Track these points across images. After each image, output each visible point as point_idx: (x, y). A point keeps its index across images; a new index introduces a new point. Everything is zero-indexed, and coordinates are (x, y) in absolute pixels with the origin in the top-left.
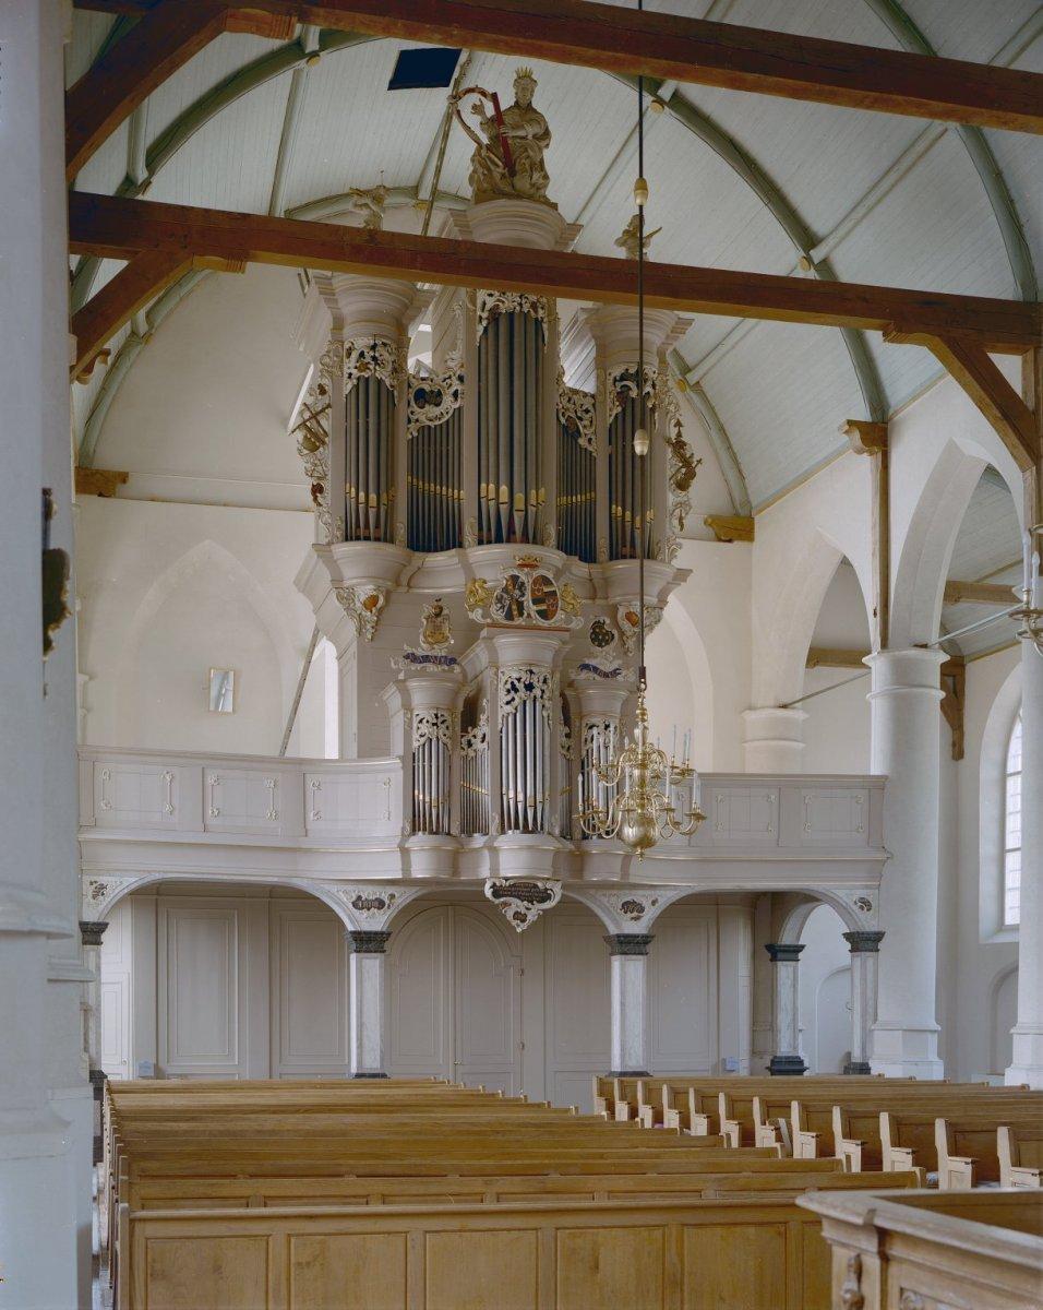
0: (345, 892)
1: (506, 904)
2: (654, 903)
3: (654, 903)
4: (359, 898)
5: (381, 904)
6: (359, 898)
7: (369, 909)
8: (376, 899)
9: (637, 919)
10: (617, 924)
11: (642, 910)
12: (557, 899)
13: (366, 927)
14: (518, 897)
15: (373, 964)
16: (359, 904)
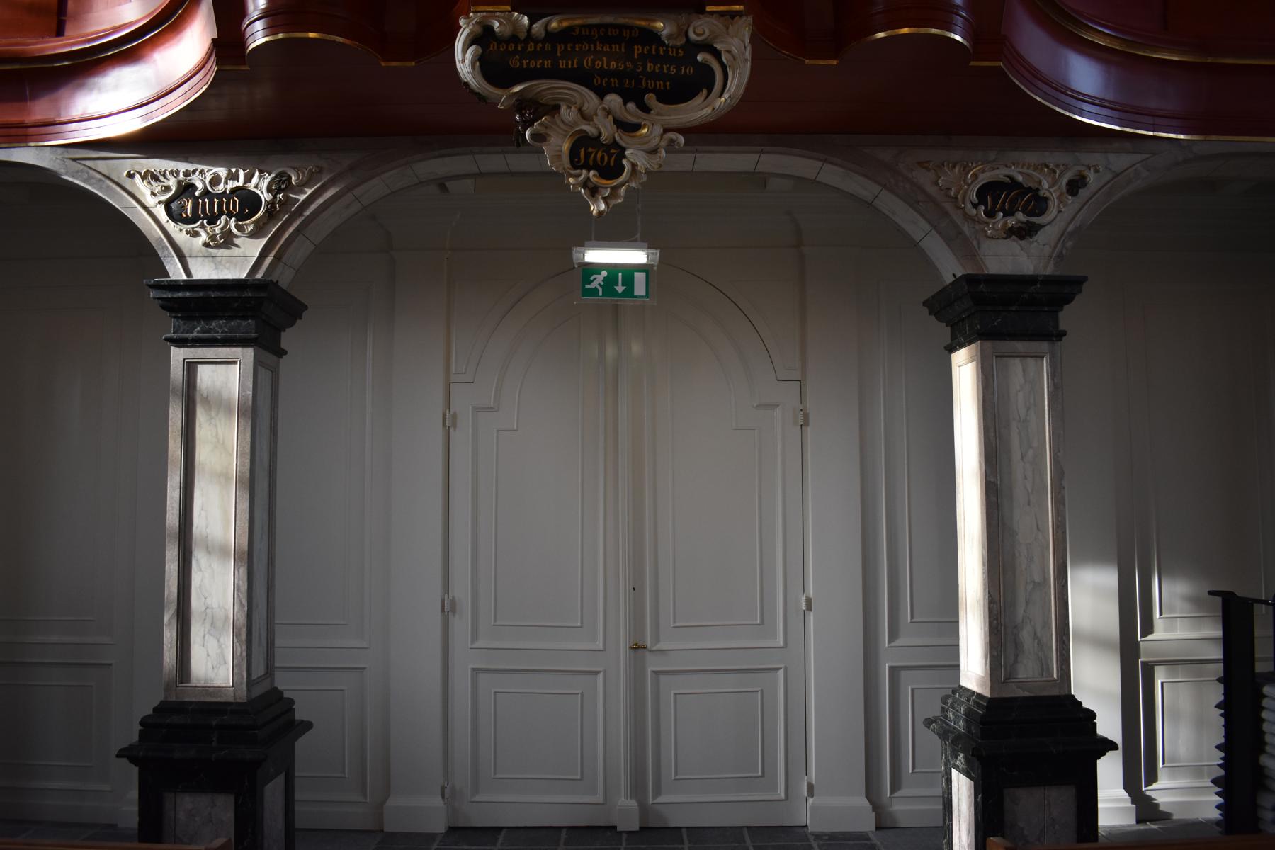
0: (151, 176)
1: (534, 108)
2: (1075, 186)
3: (1075, 186)
4: (186, 189)
5: (249, 202)
6: (186, 189)
7: (212, 220)
8: (234, 191)
9: (1025, 232)
10: (967, 250)
11: (1038, 204)
12: (737, 83)
13: (203, 271)
14: (582, 77)
15: (225, 375)
16: (186, 203)
